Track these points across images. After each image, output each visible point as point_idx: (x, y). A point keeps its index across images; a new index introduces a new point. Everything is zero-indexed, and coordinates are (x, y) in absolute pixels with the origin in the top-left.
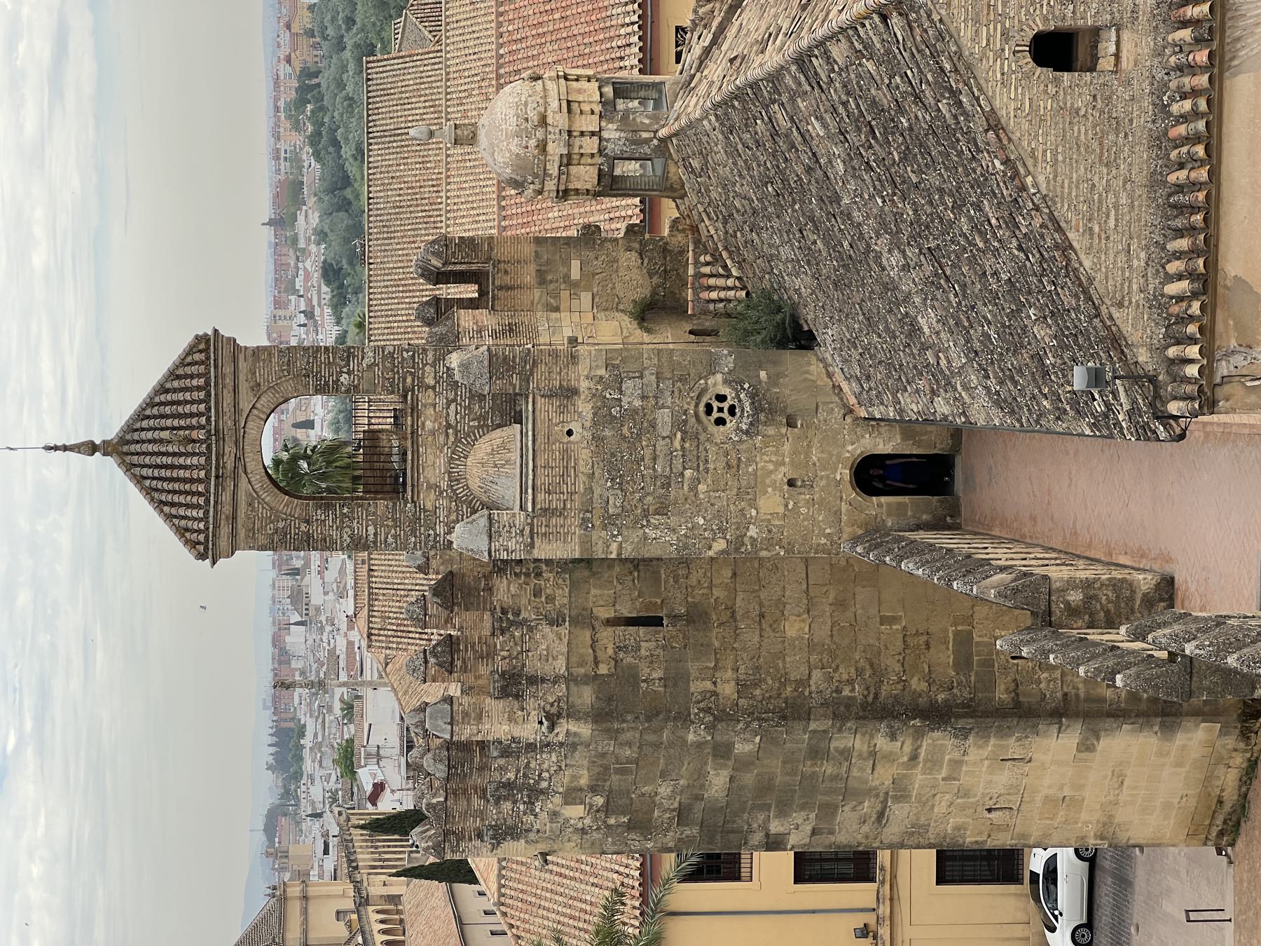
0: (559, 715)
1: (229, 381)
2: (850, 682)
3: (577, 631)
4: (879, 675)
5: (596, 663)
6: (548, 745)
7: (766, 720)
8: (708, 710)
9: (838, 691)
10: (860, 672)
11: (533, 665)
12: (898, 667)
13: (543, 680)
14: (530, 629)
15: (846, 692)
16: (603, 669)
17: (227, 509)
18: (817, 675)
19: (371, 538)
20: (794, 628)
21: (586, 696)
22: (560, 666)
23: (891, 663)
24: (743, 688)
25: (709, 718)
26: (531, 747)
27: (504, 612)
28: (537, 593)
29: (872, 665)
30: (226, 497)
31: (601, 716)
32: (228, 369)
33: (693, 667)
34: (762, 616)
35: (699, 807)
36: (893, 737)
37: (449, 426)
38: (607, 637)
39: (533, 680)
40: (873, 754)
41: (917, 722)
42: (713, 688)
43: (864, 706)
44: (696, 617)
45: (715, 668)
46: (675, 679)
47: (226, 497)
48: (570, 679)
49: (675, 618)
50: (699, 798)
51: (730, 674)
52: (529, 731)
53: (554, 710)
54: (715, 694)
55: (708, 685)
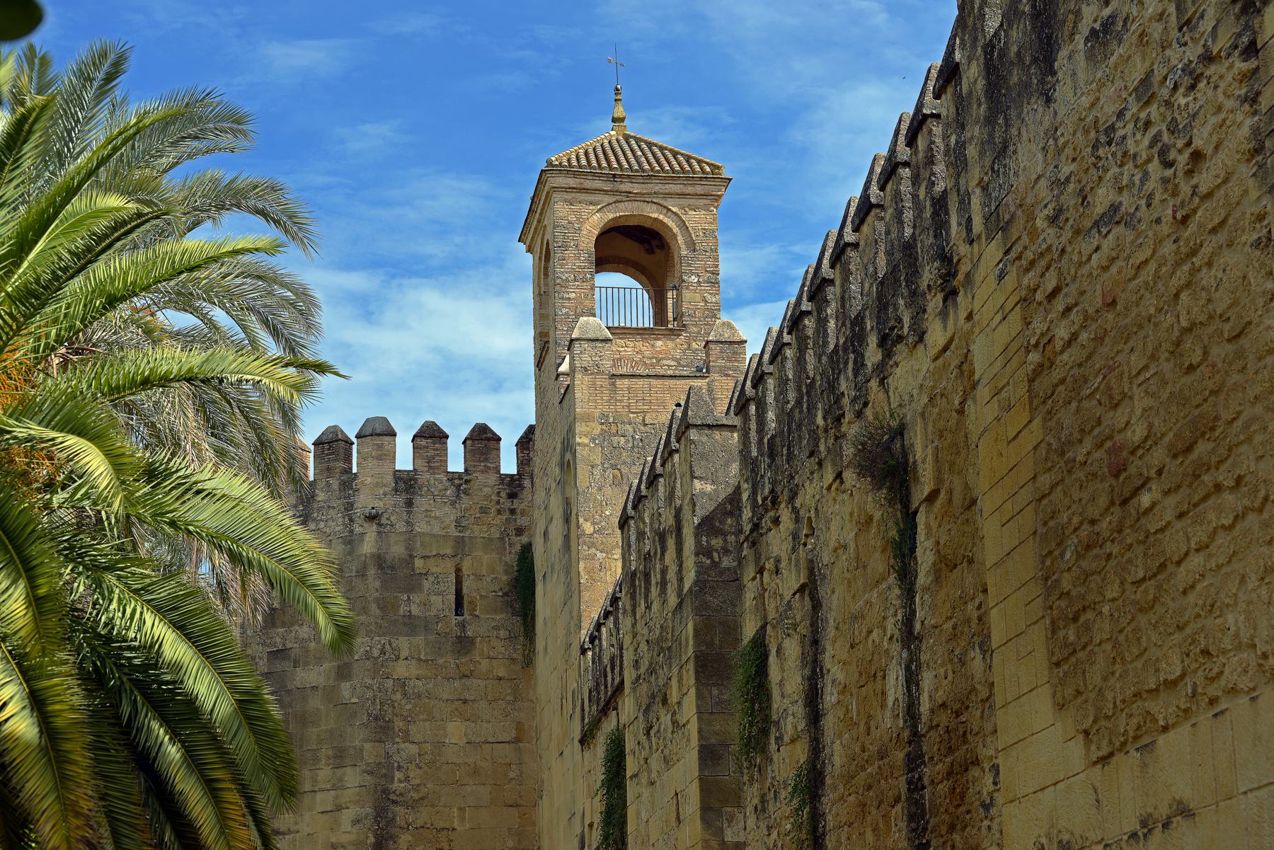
0: (380, 525)
1: (690, 190)
2: (407, 779)
3: (451, 543)
4: (413, 805)
5: (424, 557)
6: (351, 520)
7: (373, 703)
8: (383, 652)
9: (399, 768)
10: (417, 788)
11: (422, 503)
12: (420, 823)
13: (409, 513)
14: (453, 503)
15: (398, 775)
16: (418, 563)
17: (588, 184)
18: (413, 749)
19: (566, 296)
20: (455, 731)
21: (397, 550)
22: (421, 527)
23: (423, 816)
24: (402, 683)
25: (376, 653)
26: (350, 506)
27: (467, 482)
28: (484, 511)
29: (422, 799)
30: (598, 184)
31: (379, 560)
32: (699, 190)
33: (419, 640)
34: (465, 702)
35: (287, 666)
36: (356, 821)
37: (659, 360)
38: (449, 566)
39: (409, 504)
40: (339, 809)
41: (371, 840)
42: (402, 657)
43: (385, 791)
44: (464, 644)
45: (419, 660)
46: (411, 625)
47: (598, 184)
48: (410, 535)
49: (463, 626)
50: (296, 664)
51: (414, 671)
52: (365, 501)
53: (384, 521)
54: (398, 658)
55: (404, 654)
